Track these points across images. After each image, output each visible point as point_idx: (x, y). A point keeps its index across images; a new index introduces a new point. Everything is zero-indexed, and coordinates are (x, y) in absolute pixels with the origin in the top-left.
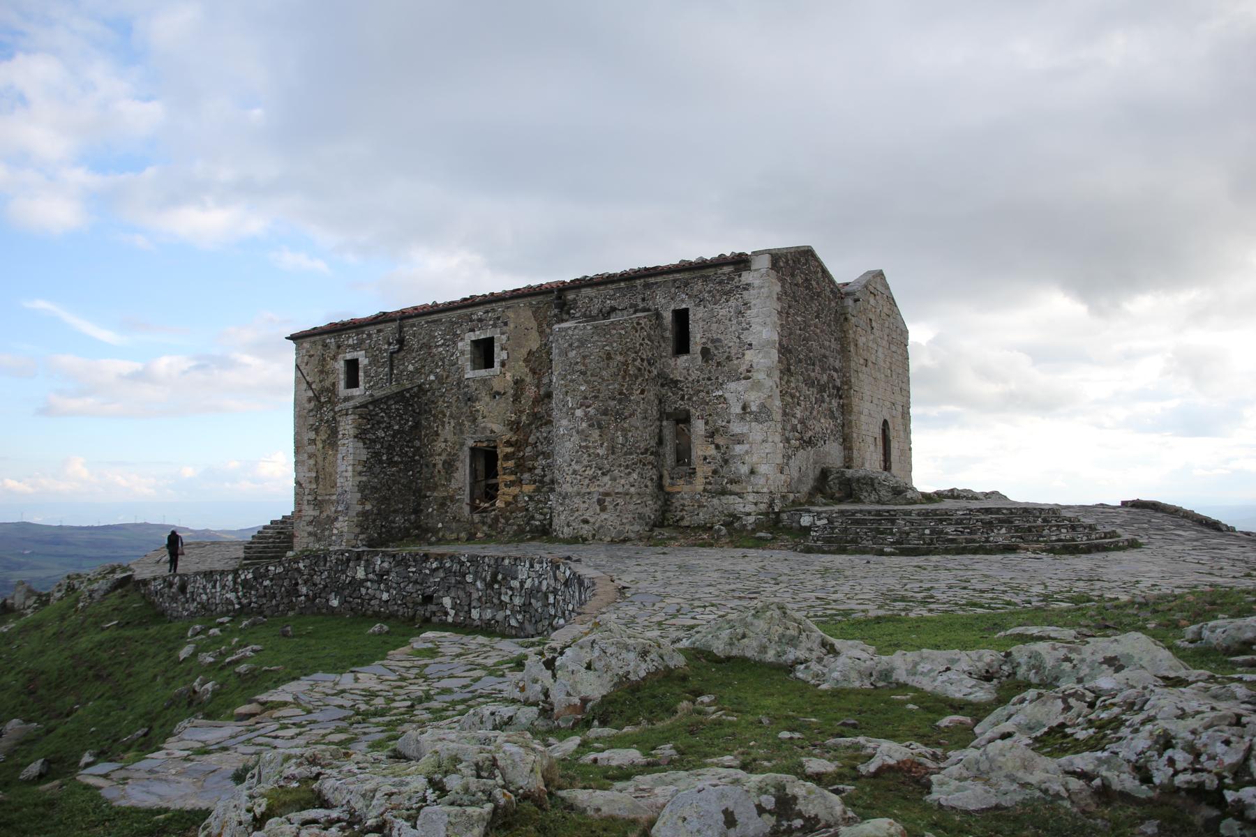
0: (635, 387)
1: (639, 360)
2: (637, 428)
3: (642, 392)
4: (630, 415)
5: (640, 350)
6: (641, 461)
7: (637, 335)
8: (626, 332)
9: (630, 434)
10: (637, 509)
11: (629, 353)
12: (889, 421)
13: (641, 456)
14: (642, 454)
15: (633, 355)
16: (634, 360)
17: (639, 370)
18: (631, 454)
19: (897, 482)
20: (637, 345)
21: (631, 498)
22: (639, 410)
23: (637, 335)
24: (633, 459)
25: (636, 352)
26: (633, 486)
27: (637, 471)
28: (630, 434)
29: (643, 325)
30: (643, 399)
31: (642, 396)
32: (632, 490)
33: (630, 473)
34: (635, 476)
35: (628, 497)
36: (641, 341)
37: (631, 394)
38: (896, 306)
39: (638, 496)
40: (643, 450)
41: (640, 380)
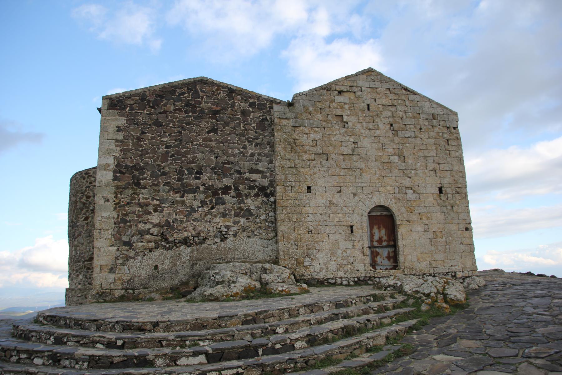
0: (81, 216)
1: (85, 198)
2: (83, 244)
3: (86, 219)
4: (78, 236)
5: (86, 191)
6: (85, 267)
7: (84, 181)
8: (76, 181)
9: (78, 248)
10: (78, 300)
11: (78, 194)
12: (394, 209)
13: (86, 263)
14: (87, 261)
15: (80, 195)
16: (81, 198)
17: (84, 204)
18: (79, 262)
19: (223, 277)
20: (84, 188)
21: (75, 293)
22: (83, 232)
23: (84, 181)
24: (80, 265)
25: (82, 193)
26: (80, 284)
27: (83, 273)
28: (78, 248)
29: (91, 174)
30: (87, 223)
31: (86, 222)
32: (80, 286)
33: (78, 276)
34: (81, 277)
35: (73, 292)
36: (88, 185)
37: (78, 221)
38: (415, 93)
39: (79, 291)
40: (87, 259)
41: (84, 211)
